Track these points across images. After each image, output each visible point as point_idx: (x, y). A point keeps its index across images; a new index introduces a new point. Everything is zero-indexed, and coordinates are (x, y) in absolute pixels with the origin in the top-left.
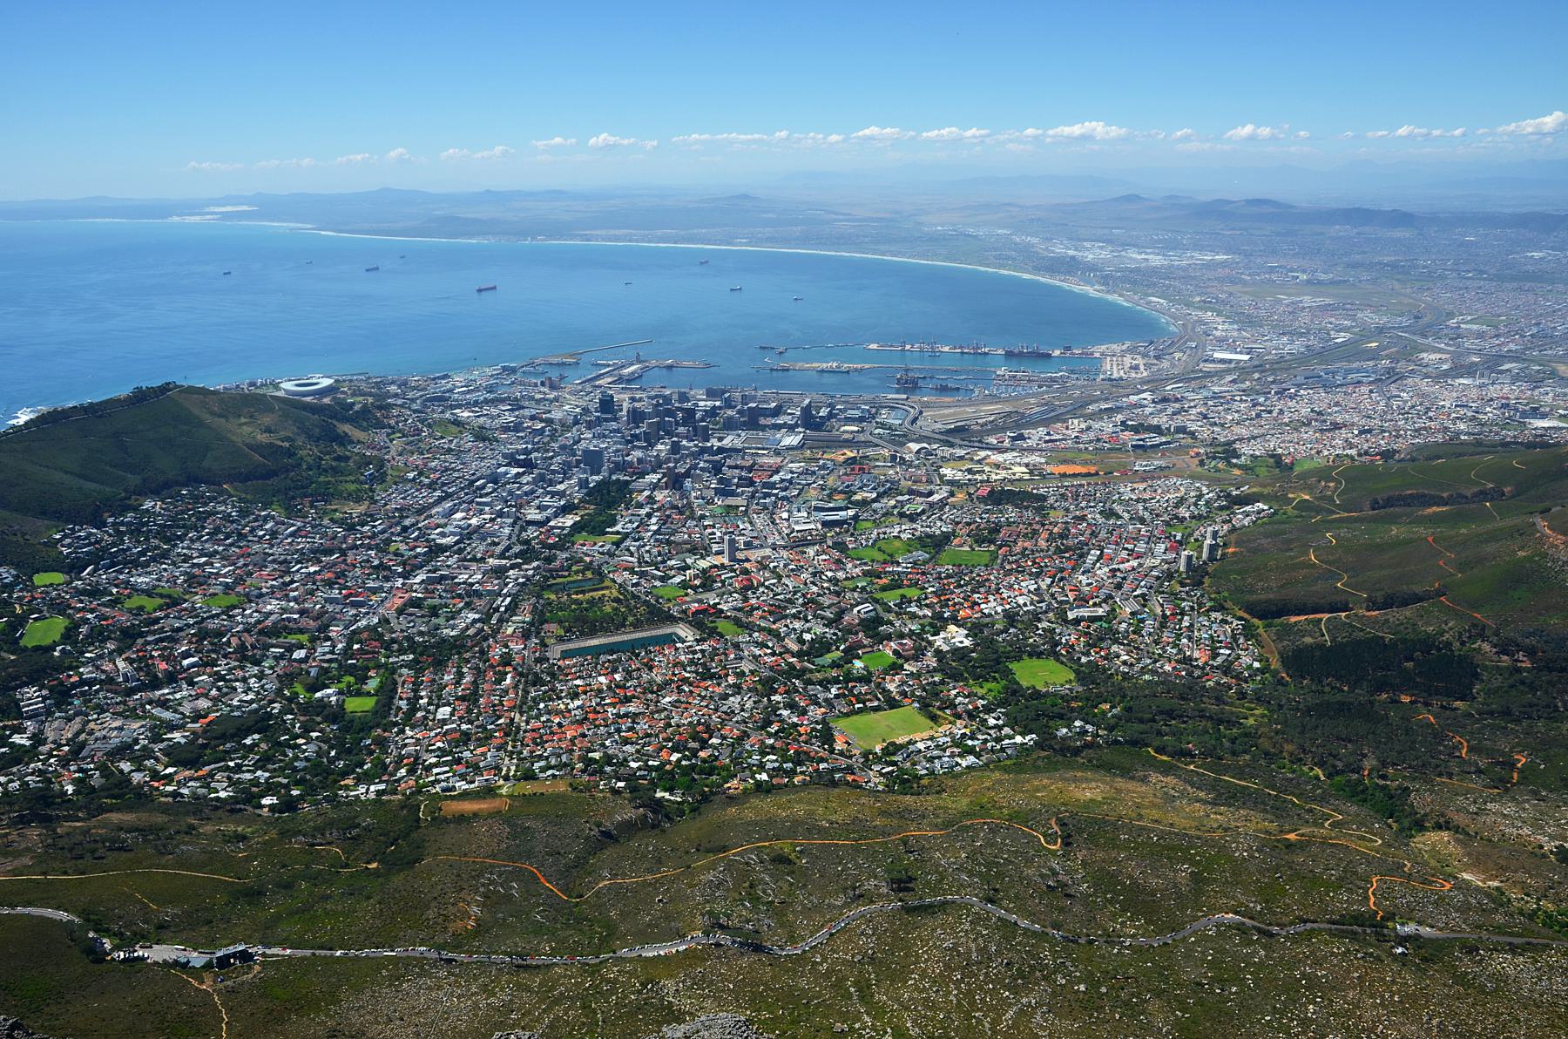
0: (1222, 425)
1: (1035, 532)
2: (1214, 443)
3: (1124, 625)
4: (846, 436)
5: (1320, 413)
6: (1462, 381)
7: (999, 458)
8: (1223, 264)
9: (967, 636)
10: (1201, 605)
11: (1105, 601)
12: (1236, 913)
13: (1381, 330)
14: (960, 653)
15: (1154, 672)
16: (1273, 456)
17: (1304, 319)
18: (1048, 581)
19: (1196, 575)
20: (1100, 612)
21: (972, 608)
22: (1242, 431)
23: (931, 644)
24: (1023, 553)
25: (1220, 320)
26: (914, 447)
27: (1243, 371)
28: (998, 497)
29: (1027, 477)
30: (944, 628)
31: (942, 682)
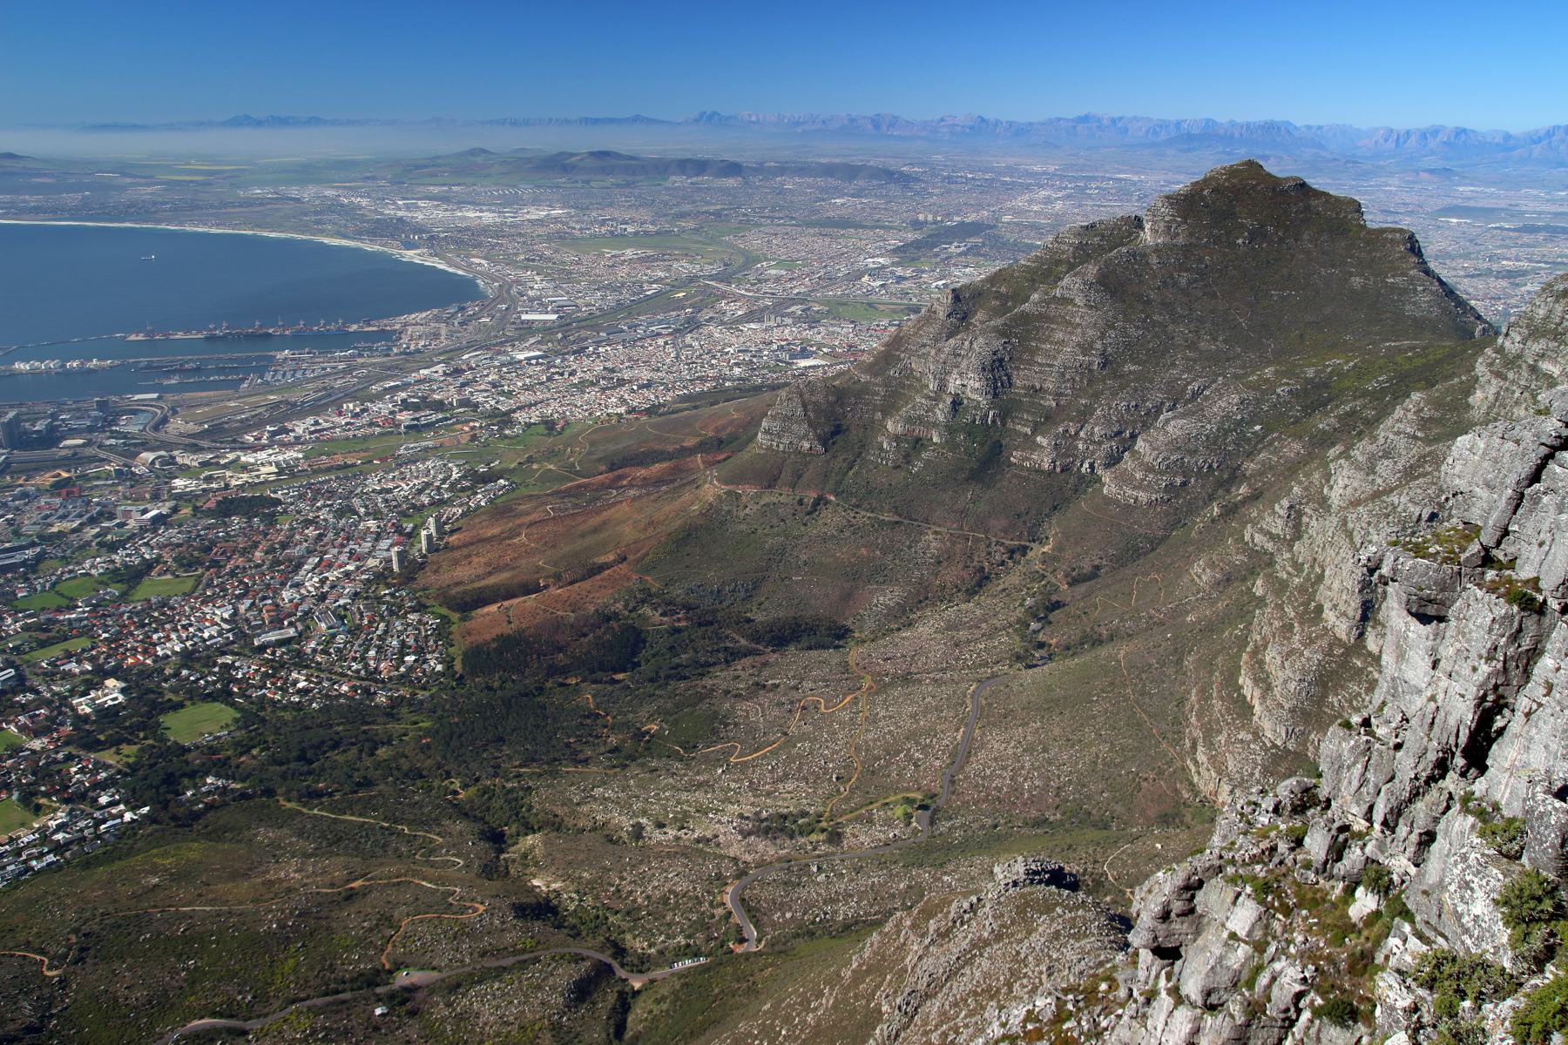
0: (509, 394)
1: (255, 545)
2: (494, 413)
3: (313, 644)
4: (63, 453)
5: (613, 371)
6: (753, 326)
7: (247, 458)
8: (556, 220)
9: (123, 691)
10: (400, 607)
11: (301, 619)
12: (214, 1015)
13: (692, 279)
14: (106, 714)
15: (327, 696)
16: (546, 423)
17: (622, 272)
18: (248, 602)
19: (411, 569)
20: (291, 632)
21: (145, 652)
22: (525, 397)
23: (73, 709)
24: (232, 574)
25: (537, 278)
26: (149, 456)
27: (547, 330)
28: (228, 506)
29: (272, 478)
30: (98, 685)
31: (69, 758)
